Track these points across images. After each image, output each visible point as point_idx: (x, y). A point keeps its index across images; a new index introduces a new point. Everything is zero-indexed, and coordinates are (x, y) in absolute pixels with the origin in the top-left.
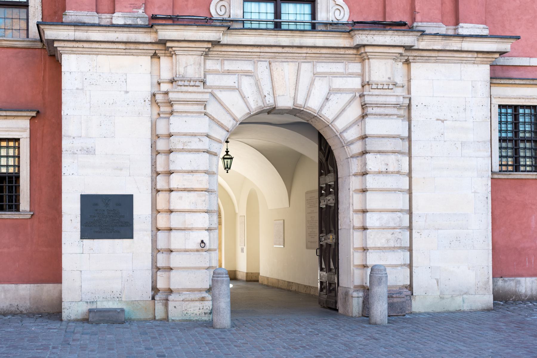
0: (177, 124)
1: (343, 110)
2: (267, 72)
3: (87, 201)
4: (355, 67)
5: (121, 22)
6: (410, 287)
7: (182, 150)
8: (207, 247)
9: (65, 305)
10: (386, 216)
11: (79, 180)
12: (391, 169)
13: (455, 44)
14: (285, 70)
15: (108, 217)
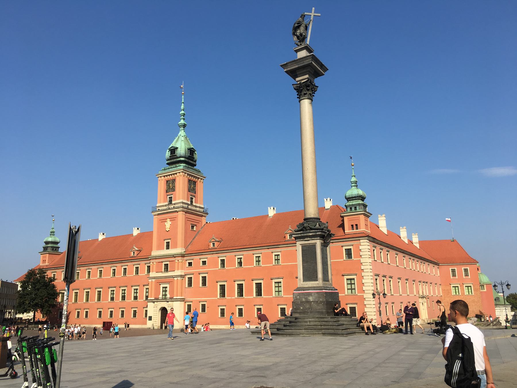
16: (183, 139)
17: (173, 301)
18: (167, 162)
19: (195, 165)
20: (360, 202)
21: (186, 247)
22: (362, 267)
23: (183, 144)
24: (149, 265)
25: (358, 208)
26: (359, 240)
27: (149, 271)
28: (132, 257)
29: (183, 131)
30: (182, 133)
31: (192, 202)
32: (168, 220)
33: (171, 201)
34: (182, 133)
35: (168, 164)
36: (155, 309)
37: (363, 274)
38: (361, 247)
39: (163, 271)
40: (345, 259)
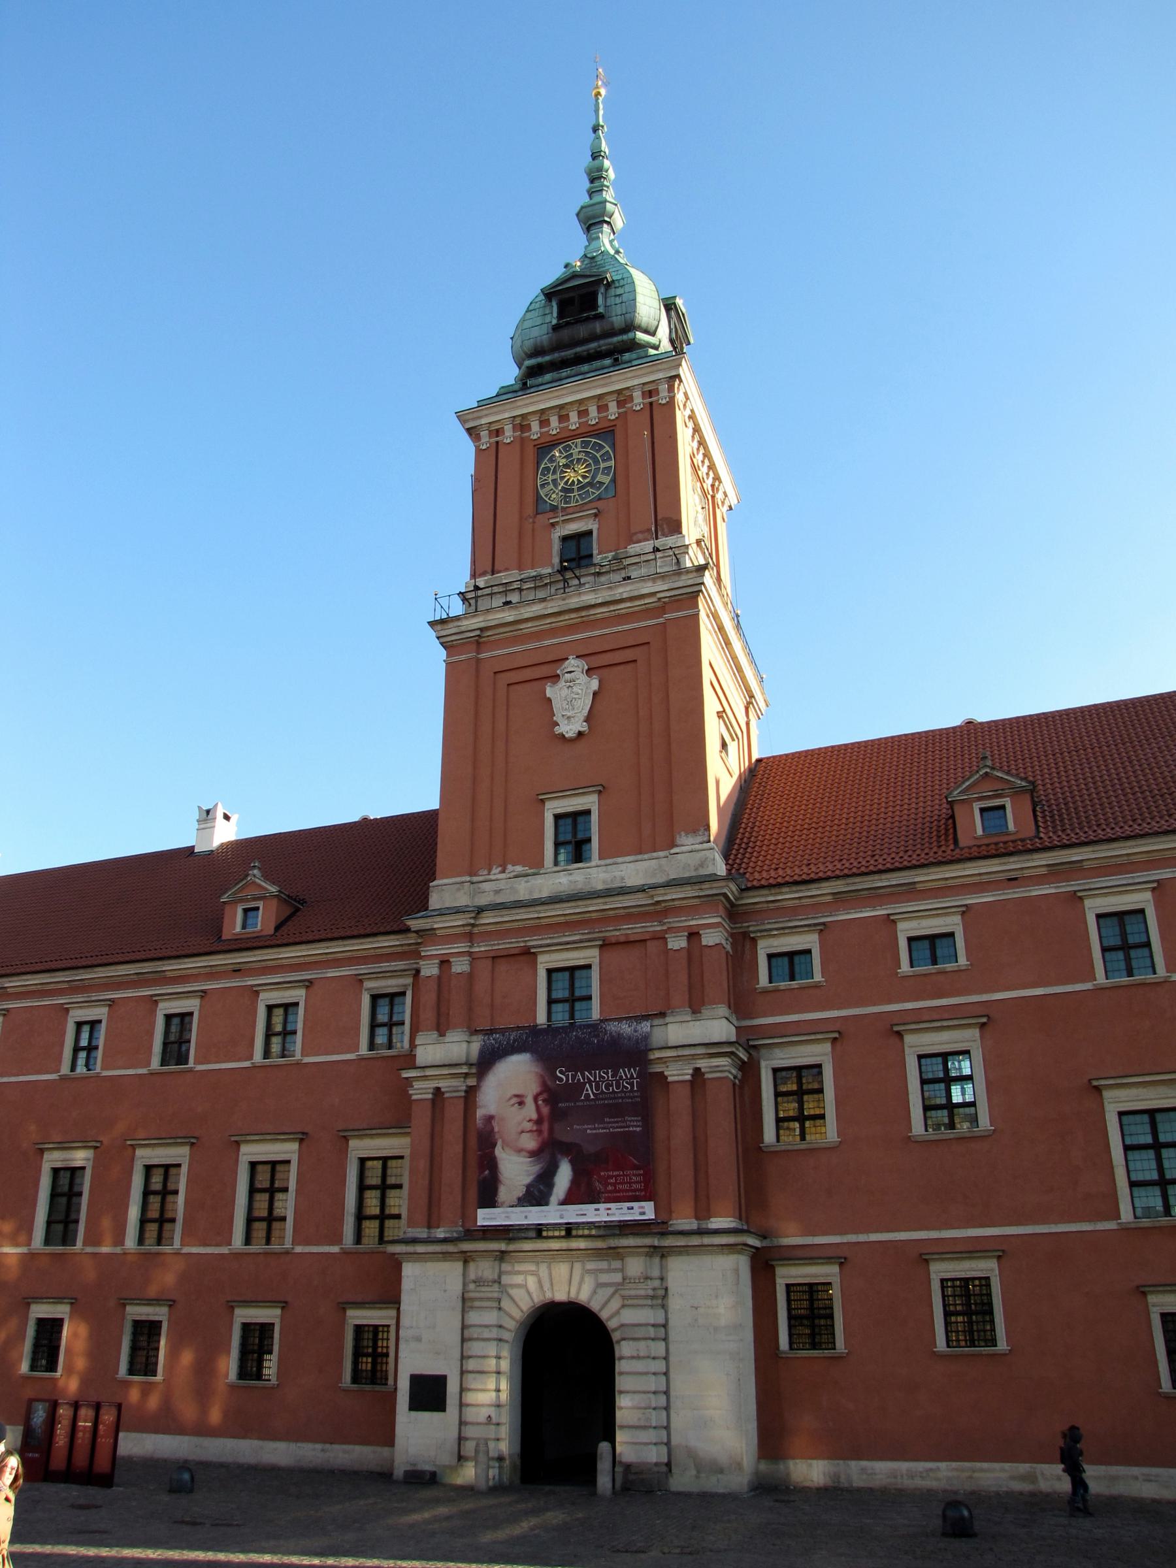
0: (474, 1318)
1: (608, 1301)
2: (547, 1271)
3: (417, 1381)
4: (616, 1264)
5: (442, 1236)
6: (668, 1465)
7: (477, 1339)
8: (494, 1420)
9: (396, 1464)
10: (637, 1397)
11: (411, 1361)
12: (642, 1354)
13: (695, 1241)
14: (561, 1269)
15: (430, 1393)
17: (662, 1253)
24: (390, 985)
32: (573, 663)
36: (490, 1317)
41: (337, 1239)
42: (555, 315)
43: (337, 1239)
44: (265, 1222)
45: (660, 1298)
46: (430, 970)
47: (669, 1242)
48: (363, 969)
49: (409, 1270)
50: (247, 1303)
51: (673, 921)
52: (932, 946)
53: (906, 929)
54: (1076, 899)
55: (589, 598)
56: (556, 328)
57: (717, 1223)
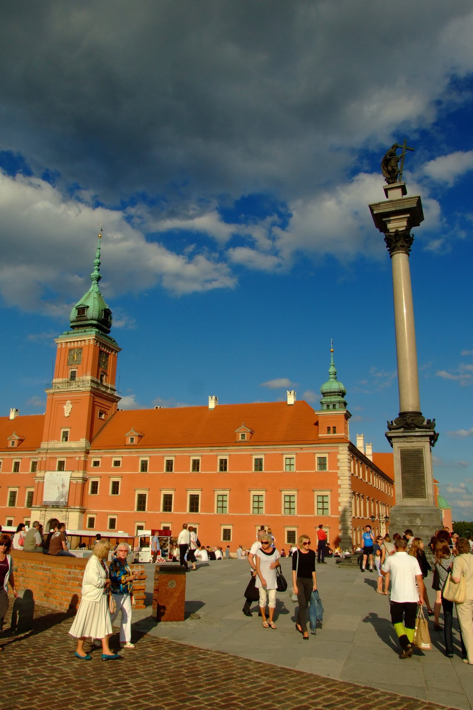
14: (54, 513)
16: (96, 295)
17: (69, 511)
18: (72, 324)
19: (109, 332)
20: (339, 398)
21: (90, 438)
22: (339, 482)
23: (96, 302)
24: (35, 460)
25: (337, 406)
26: (338, 447)
27: (34, 469)
28: (10, 448)
29: (96, 286)
30: (94, 288)
31: (101, 380)
32: (68, 402)
33: (73, 376)
34: (94, 288)
35: (73, 327)
37: (340, 491)
38: (339, 457)
39: (57, 469)
40: (316, 470)
41: (23, 506)
42: (77, 313)
43: (23, 506)
44: (12, 503)
45: (67, 518)
46: (40, 459)
47: (69, 510)
48: (31, 457)
49: (32, 512)
50: (8, 517)
51: (77, 455)
52: (117, 463)
53: (115, 459)
54: (139, 457)
55: (71, 389)
56: (77, 317)
57: (77, 507)
